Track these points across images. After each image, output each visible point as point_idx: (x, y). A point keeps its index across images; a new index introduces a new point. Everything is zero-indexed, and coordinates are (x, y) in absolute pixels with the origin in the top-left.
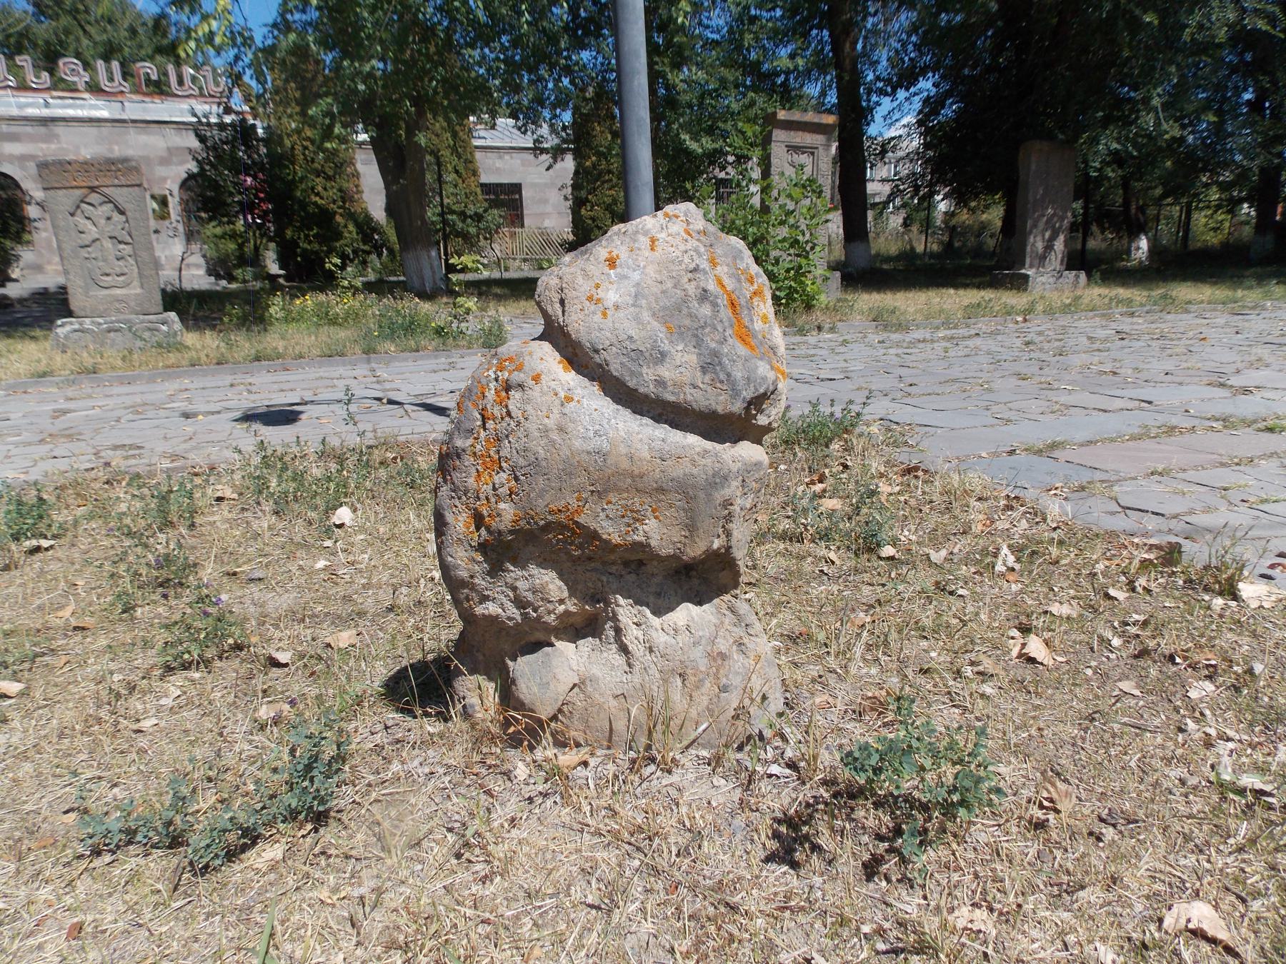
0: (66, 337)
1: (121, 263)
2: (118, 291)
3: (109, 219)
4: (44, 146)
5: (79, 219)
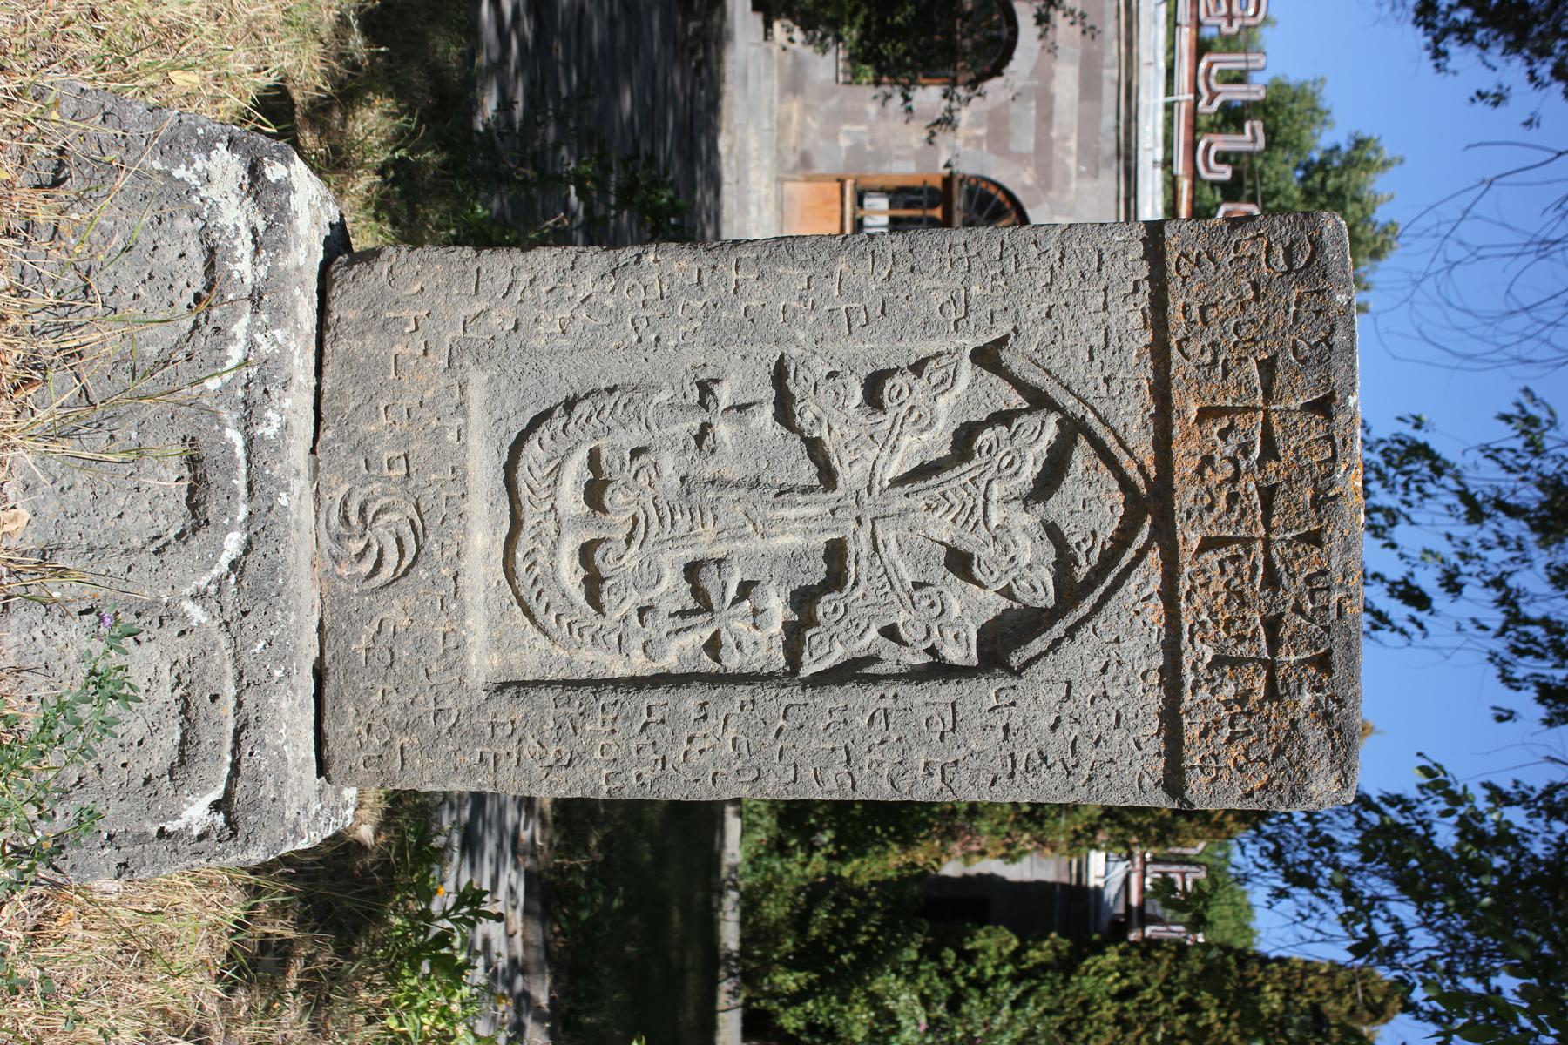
1: (671, 589)
2: (482, 539)
3: (960, 563)
4: (1073, 144)
5: (969, 392)
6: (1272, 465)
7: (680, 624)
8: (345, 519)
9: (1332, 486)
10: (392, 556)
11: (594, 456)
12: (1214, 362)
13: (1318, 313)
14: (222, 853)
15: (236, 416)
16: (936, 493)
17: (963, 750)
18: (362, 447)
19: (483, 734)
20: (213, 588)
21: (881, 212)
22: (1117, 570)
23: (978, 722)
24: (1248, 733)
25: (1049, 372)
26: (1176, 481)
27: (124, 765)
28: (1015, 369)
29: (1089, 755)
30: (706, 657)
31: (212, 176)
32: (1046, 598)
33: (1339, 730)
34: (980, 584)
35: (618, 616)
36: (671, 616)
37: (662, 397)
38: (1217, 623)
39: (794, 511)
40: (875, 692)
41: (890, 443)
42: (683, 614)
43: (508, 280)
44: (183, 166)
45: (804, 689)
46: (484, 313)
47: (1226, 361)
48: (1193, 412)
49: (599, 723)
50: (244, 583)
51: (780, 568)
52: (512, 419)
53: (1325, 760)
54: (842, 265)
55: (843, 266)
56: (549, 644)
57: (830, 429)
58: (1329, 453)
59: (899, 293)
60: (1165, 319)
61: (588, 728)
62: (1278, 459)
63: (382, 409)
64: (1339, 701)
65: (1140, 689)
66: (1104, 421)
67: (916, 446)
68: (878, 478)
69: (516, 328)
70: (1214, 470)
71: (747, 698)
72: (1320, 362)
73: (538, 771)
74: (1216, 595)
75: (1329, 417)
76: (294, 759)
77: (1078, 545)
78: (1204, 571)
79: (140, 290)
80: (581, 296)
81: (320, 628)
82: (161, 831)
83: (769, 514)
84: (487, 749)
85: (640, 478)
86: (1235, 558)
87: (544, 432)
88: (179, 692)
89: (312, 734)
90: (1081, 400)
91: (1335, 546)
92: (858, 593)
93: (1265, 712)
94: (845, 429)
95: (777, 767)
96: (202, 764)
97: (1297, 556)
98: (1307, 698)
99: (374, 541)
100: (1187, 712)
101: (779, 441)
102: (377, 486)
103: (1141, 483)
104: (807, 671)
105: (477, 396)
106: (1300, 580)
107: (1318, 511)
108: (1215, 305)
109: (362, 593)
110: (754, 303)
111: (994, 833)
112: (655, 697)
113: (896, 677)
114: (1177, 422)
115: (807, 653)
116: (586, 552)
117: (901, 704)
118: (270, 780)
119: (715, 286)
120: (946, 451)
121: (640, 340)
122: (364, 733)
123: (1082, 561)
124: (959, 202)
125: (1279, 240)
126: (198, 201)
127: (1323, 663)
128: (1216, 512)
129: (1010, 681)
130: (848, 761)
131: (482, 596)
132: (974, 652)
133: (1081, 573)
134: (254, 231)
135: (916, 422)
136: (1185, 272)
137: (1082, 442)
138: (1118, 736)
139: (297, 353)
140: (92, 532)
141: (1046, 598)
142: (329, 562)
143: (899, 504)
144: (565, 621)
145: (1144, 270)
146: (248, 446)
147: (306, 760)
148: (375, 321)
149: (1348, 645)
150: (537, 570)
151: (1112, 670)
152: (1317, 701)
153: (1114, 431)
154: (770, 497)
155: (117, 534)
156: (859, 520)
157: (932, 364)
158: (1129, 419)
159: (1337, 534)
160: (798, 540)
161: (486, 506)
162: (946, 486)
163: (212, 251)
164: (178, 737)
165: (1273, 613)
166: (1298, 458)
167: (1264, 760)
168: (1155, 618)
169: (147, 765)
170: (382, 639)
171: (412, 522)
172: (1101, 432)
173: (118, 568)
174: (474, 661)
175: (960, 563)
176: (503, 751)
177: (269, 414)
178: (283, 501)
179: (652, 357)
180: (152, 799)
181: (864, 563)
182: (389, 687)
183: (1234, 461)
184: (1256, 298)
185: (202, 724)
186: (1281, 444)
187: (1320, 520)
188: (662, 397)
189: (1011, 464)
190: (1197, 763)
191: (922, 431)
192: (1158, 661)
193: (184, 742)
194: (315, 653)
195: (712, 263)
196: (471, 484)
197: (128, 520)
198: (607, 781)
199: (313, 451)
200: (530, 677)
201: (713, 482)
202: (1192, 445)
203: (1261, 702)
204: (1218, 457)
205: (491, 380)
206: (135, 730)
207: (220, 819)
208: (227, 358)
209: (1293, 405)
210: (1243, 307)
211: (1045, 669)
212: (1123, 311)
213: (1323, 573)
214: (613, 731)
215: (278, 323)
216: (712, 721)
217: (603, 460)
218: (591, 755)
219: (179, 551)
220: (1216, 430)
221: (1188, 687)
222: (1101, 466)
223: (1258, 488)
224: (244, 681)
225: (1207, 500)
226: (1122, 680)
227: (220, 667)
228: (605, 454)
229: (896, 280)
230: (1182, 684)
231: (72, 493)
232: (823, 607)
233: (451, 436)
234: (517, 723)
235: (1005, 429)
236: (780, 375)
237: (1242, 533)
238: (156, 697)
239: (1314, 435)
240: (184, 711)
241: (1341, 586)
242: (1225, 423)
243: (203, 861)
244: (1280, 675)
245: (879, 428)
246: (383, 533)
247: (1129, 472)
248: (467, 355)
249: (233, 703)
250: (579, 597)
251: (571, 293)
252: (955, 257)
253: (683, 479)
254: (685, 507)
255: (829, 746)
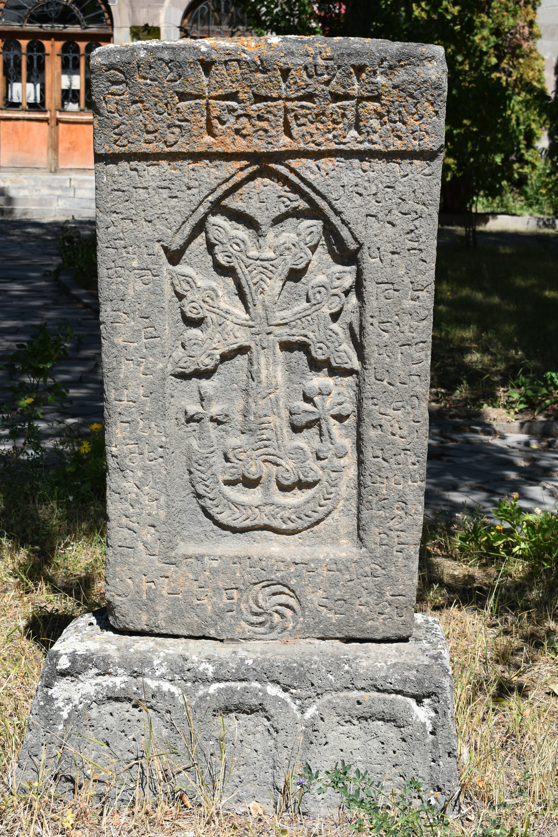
0: (77, 715)
1: (306, 441)
2: (275, 547)
3: (295, 275)
5: (195, 269)
6: (241, 96)
7: (326, 437)
8: (261, 624)
9: (254, 62)
10: (283, 599)
11: (228, 483)
12: (180, 127)
13: (151, 67)
14: (445, 701)
15: (201, 687)
16: (254, 288)
17: (404, 278)
18: (220, 614)
19: (386, 551)
20: (298, 702)
21: (24, 89)
22: (302, 185)
23: (389, 270)
24: (400, 112)
25: (184, 223)
26: (250, 150)
27: (394, 752)
28: (181, 242)
29: (410, 205)
30: (346, 423)
31: (67, 697)
32: (317, 225)
33: (399, 61)
34: (307, 265)
35: (321, 472)
36: (322, 441)
37: (195, 443)
38: (334, 129)
39: (262, 371)
40: (369, 329)
41: (224, 314)
42: (321, 435)
43: (126, 530)
44: (61, 713)
45: (366, 369)
46: (145, 544)
47: (179, 120)
48: (208, 139)
49: (382, 485)
50: (296, 685)
51: (296, 379)
52: (206, 528)
53: (417, 69)
54: (119, 341)
55: (120, 340)
56: (336, 511)
57: (215, 349)
58: (235, 63)
59: (136, 309)
60: (154, 154)
61: (384, 492)
62: (238, 92)
63: (199, 602)
64: (382, 61)
65: (372, 174)
66: (213, 191)
67: (226, 298)
68: (244, 322)
69: (154, 526)
70: (243, 129)
71: (370, 402)
72: (181, 67)
73: (408, 520)
74: (317, 129)
75: (213, 63)
76: (396, 657)
77: (286, 206)
78: (303, 135)
79: (131, 737)
80: (136, 490)
81: (323, 639)
82: (432, 733)
83: (264, 385)
84: (395, 549)
85: (241, 457)
86: (296, 117)
87: (213, 511)
88: (355, 722)
89: (383, 645)
90: (200, 203)
91: (289, 61)
92: (311, 335)
93: (387, 103)
94: (216, 340)
95: (411, 385)
96: (395, 710)
97: (295, 83)
98: (380, 79)
99: (274, 609)
100: (387, 147)
101: (221, 377)
102: (243, 606)
103: (250, 170)
104: (356, 364)
105: (191, 549)
106: (310, 81)
107: (269, 70)
108: (145, 125)
109: (303, 615)
110: (141, 391)
111: (514, 16)
112: (368, 454)
113: (361, 314)
114: (215, 149)
115: (345, 366)
116: (283, 488)
117: (376, 314)
118: (406, 673)
119: (131, 413)
120: (230, 281)
121: (162, 457)
122: (383, 616)
123: (295, 204)
124: (16, 26)
125: (107, 88)
126: (82, 705)
127: (359, 69)
128: (269, 128)
129: (365, 249)
130: (409, 345)
131: (307, 548)
132: (347, 268)
133: (303, 204)
134: (98, 675)
135: (212, 299)
136: (125, 142)
137: (225, 202)
138: (399, 188)
139: (166, 651)
140: (265, 766)
141: (317, 225)
142: (285, 633)
143: (260, 310)
144: (323, 502)
145: (124, 165)
146: (219, 680)
147: (397, 650)
148: (149, 604)
149: (349, 55)
150: (293, 517)
151: (361, 190)
152: (382, 73)
153: (219, 185)
154: (254, 384)
155: (266, 753)
156: (269, 334)
157: (178, 289)
158: (212, 176)
159: (283, 60)
160: (279, 368)
161: (255, 544)
162: (250, 283)
163: (109, 698)
164: (381, 723)
165: (329, 97)
166: (238, 81)
167: (416, 104)
168: (330, 164)
169: (395, 740)
170: (330, 605)
171: (263, 587)
172: (219, 192)
173: (285, 753)
174: (344, 554)
175: (295, 275)
176: (396, 540)
177: (201, 669)
178: (250, 662)
179: (171, 450)
180: (414, 738)
181: (294, 331)
182: (358, 602)
183: (238, 117)
184: (142, 102)
185: (373, 710)
186: (229, 90)
187: (275, 69)
188: (195, 443)
189: (238, 244)
190: (417, 142)
191: (217, 296)
192: (356, 162)
193: (383, 719)
194: (337, 643)
195: (117, 415)
196: (243, 554)
197: (258, 747)
198: (416, 482)
199: (222, 641)
200: (355, 522)
201: (245, 416)
202: (228, 140)
203: (382, 105)
204: (236, 126)
205: (182, 540)
206: (375, 746)
207: (426, 701)
208: (169, 691)
209: (206, 83)
210: (147, 110)
211: (359, 229)
212: (148, 178)
213: (306, 68)
214: (387, 478)
215: (150, 663)
216: (383, 422)
217: (231, 478)
218: (400, 491)
219: (277, 720)
220: (220, 126)
221: (372, 147)
222: (240, 191)
223: (255, 103)
224: (350, 686)
225: (261, 133)
226: (367, 184)
227: (342, 699)
228: (227, 477)
229: (128, 310)
230: (370, 150)
231: (243, 777)
232: (319, 355)
233: (215, 564)
234: (381, 531)
235: (217, 247)
236: (183, 376)
237: (281, 113)
238: (357, 734)
239: (224, 72)
240: (366, 719)
241: (314, 58)
242: (215, 122)
243: (449, 711)
244: (366, 94)
245: (215, 321)
246: (270, 603)
247: (244, 176)
248: (168, 554)
249: (362, 693)
250: (310, 493)
251: (134, 495)
252: (116, 275)
253: (243, 433)
254: (259, 432)
255: (400, 356)
